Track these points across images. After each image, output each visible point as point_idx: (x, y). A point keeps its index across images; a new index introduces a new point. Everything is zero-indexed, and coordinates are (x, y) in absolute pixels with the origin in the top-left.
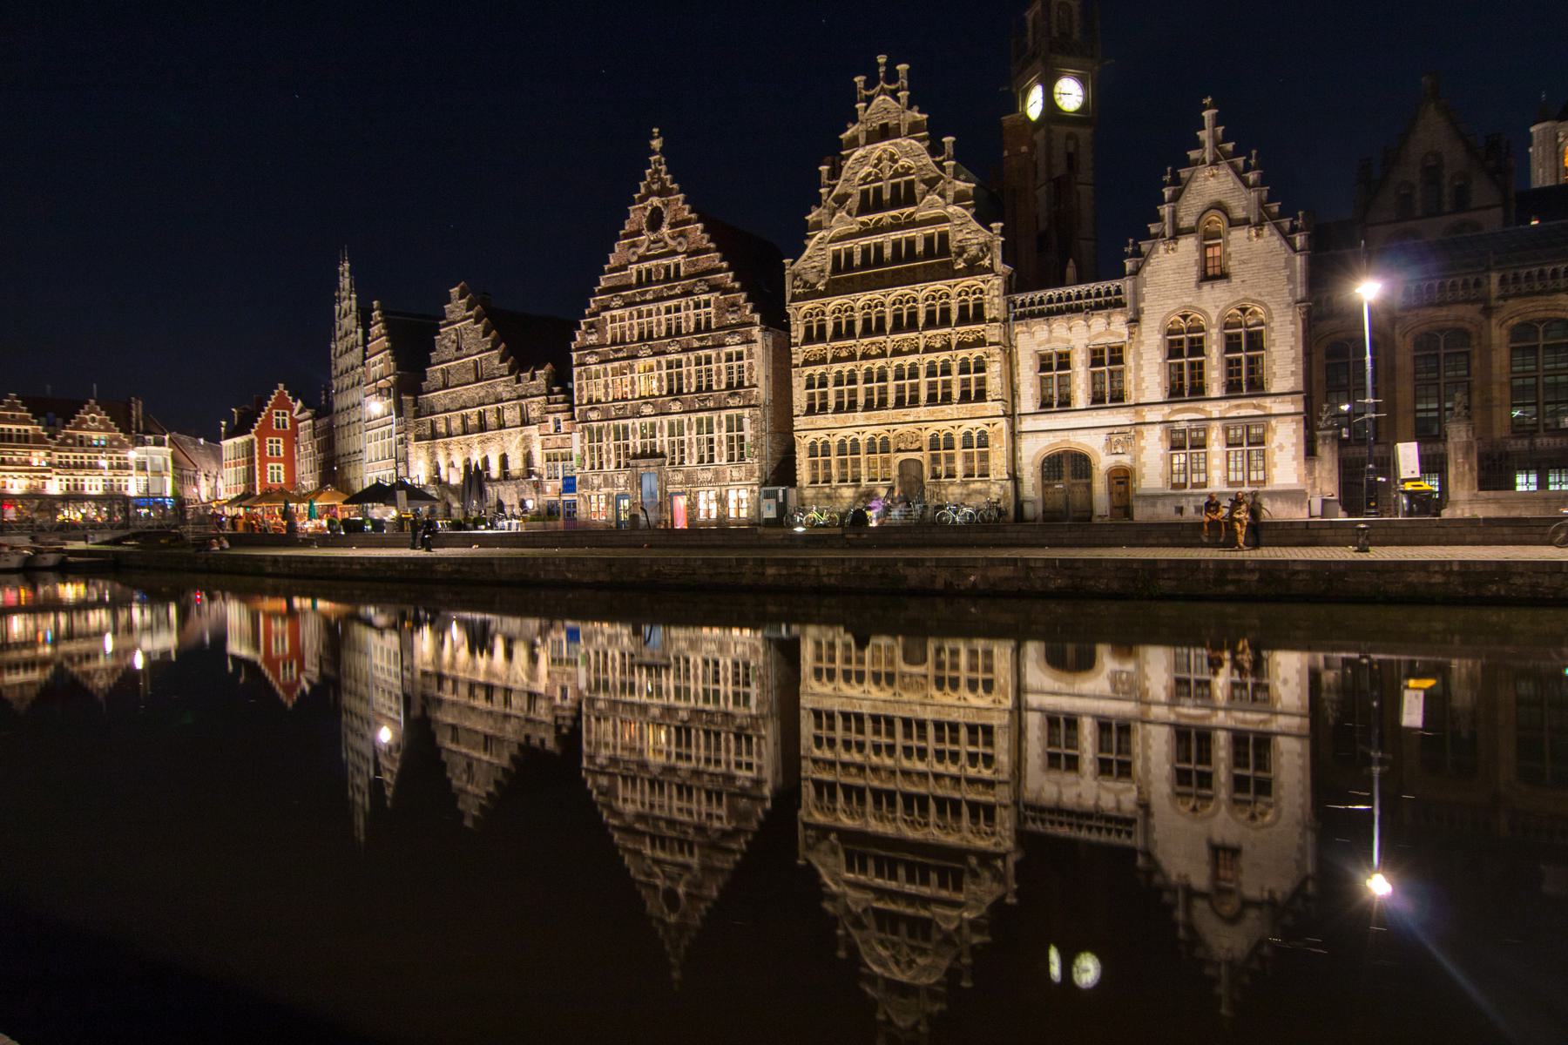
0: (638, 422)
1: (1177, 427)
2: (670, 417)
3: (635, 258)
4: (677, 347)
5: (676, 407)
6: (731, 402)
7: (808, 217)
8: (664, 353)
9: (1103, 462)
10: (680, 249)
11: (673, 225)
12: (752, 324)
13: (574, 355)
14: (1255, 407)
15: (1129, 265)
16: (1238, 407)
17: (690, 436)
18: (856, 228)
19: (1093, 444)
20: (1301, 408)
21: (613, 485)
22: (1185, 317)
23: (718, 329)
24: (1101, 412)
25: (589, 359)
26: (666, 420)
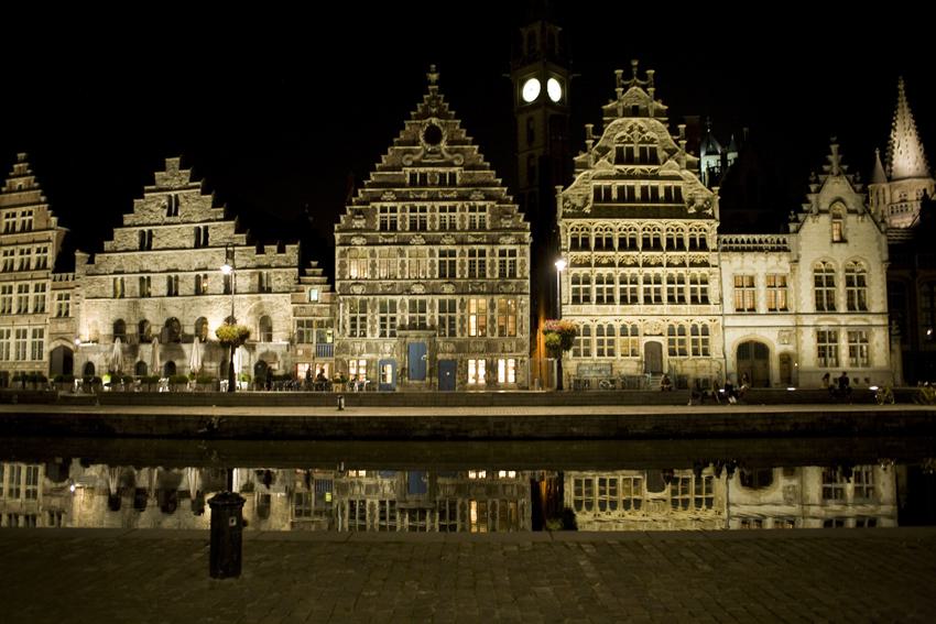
0: (407, 299)
1: (822, 329)
2: (441, 297)
3: (410, 163)
5: (448, 289)
7: (576, 159)
8: (438, 243)
9: (777, 349)
10: (456, 162)
11: (450, 143)
12: (524, 230)
13: (337, 236)
14: (865, 320)
15: (792, 227)
16: (855, 319)
18: (614, 172)
20: (887, 322)
21: (377, 351)
22: (824, 263)
23: (492, 230)
24: (776, 317)
25: (355, 240)
26: (437, 299)
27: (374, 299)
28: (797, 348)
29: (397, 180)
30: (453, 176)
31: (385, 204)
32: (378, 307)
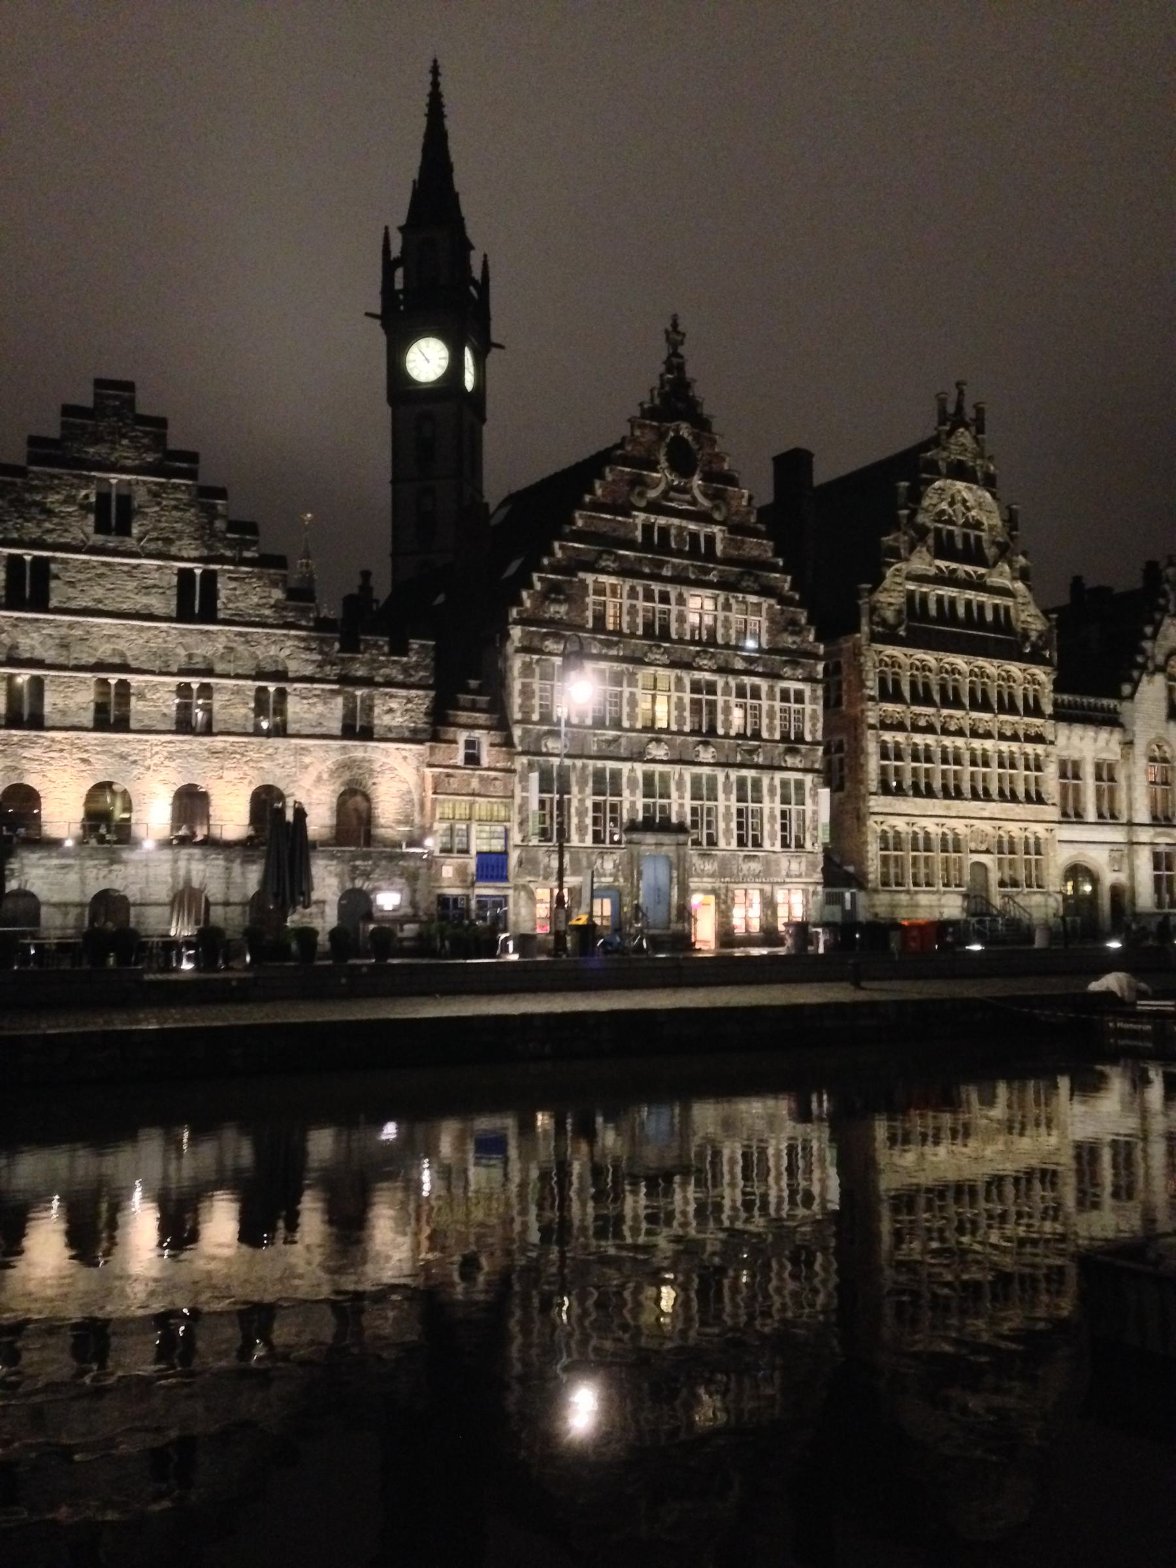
0: (640, 768)
1: (1160, 849)
3: (643, 504)
4: (665, 659)
5: (707, 755)
6: (790, 761)
7: (884, 539)
8: (688, 666)
10: (717, 516)
13: (516, 632)
15: (1126, 689)
17: (726, 803)
18: (932, 571)
19: (1098, 858)
22: (1159, 747)
24: (1106, 828)
25: (550, 645)
26: (688, 772)
27: (584, 767)
28: (1132, 877)
29: (621, 532)
30: (711, 539)
31: (603, 578)
32: (591, 784)
